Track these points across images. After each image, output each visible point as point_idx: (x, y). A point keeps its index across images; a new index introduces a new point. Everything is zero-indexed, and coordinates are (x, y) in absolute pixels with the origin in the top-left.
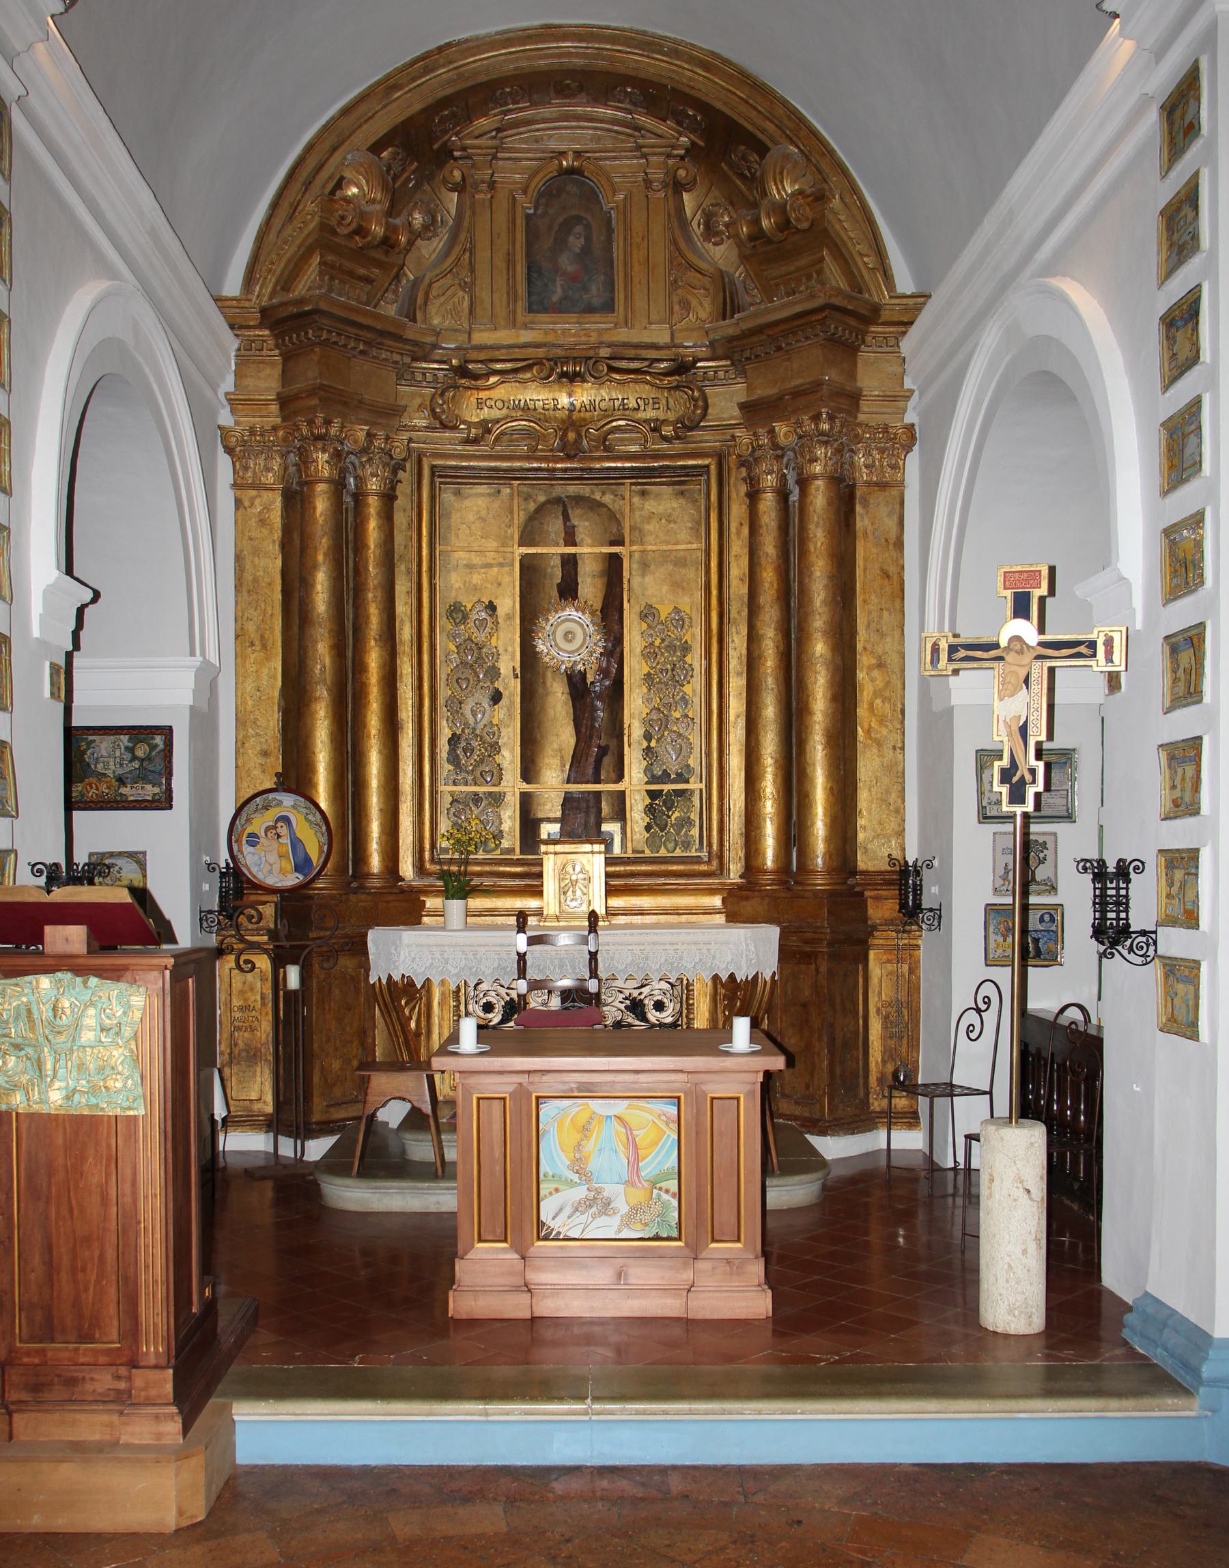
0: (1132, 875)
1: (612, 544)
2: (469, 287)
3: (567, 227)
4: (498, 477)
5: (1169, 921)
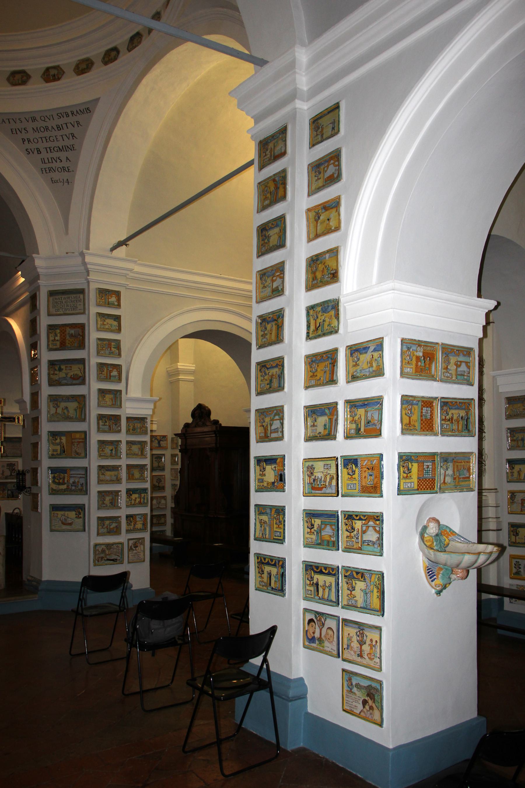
0: (26, 474)
5: (33, 485)
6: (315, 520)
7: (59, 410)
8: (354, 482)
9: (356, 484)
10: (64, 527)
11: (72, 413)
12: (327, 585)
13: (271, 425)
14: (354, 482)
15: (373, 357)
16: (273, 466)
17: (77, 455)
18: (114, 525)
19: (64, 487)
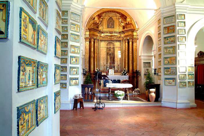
1: (113, 46)
2: (103, 26)
3: (110, 22)
4: (105, 41)
7: (167, 51)
10: (169, 84)
11: (171, 52)
17: (173, 64)
18: (185, 84)
19: (169, 73)
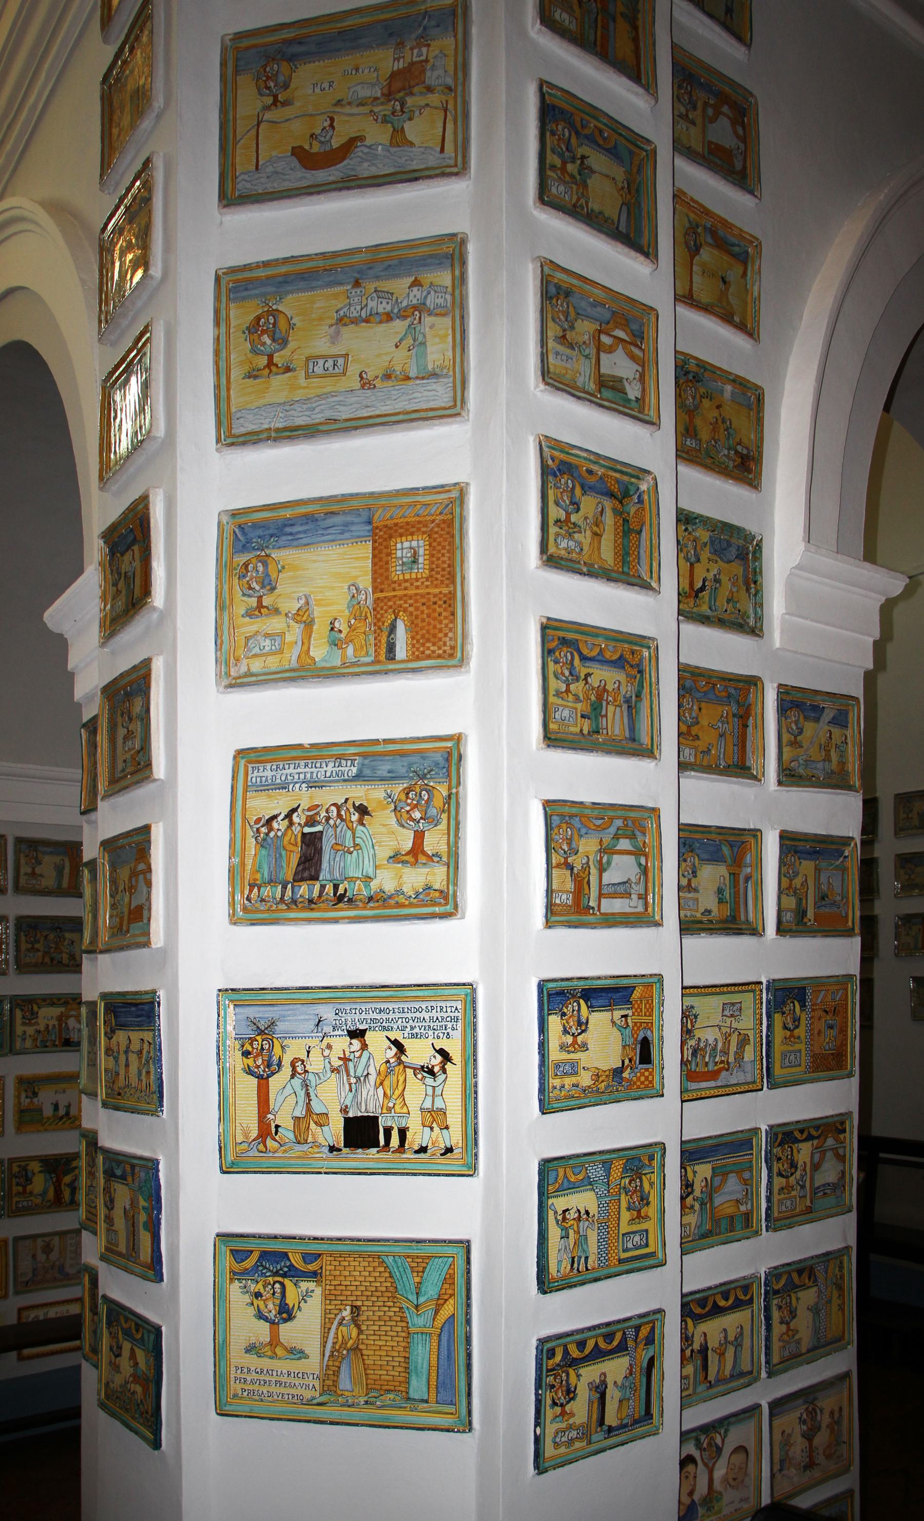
6: (697, 1168)
8: (797, 1047)
9: (800, 1051)
12: (731, 1338)
13: (602, 870)
14: (797, 1047)
15: (830, 737)
16: (617, 1014)
